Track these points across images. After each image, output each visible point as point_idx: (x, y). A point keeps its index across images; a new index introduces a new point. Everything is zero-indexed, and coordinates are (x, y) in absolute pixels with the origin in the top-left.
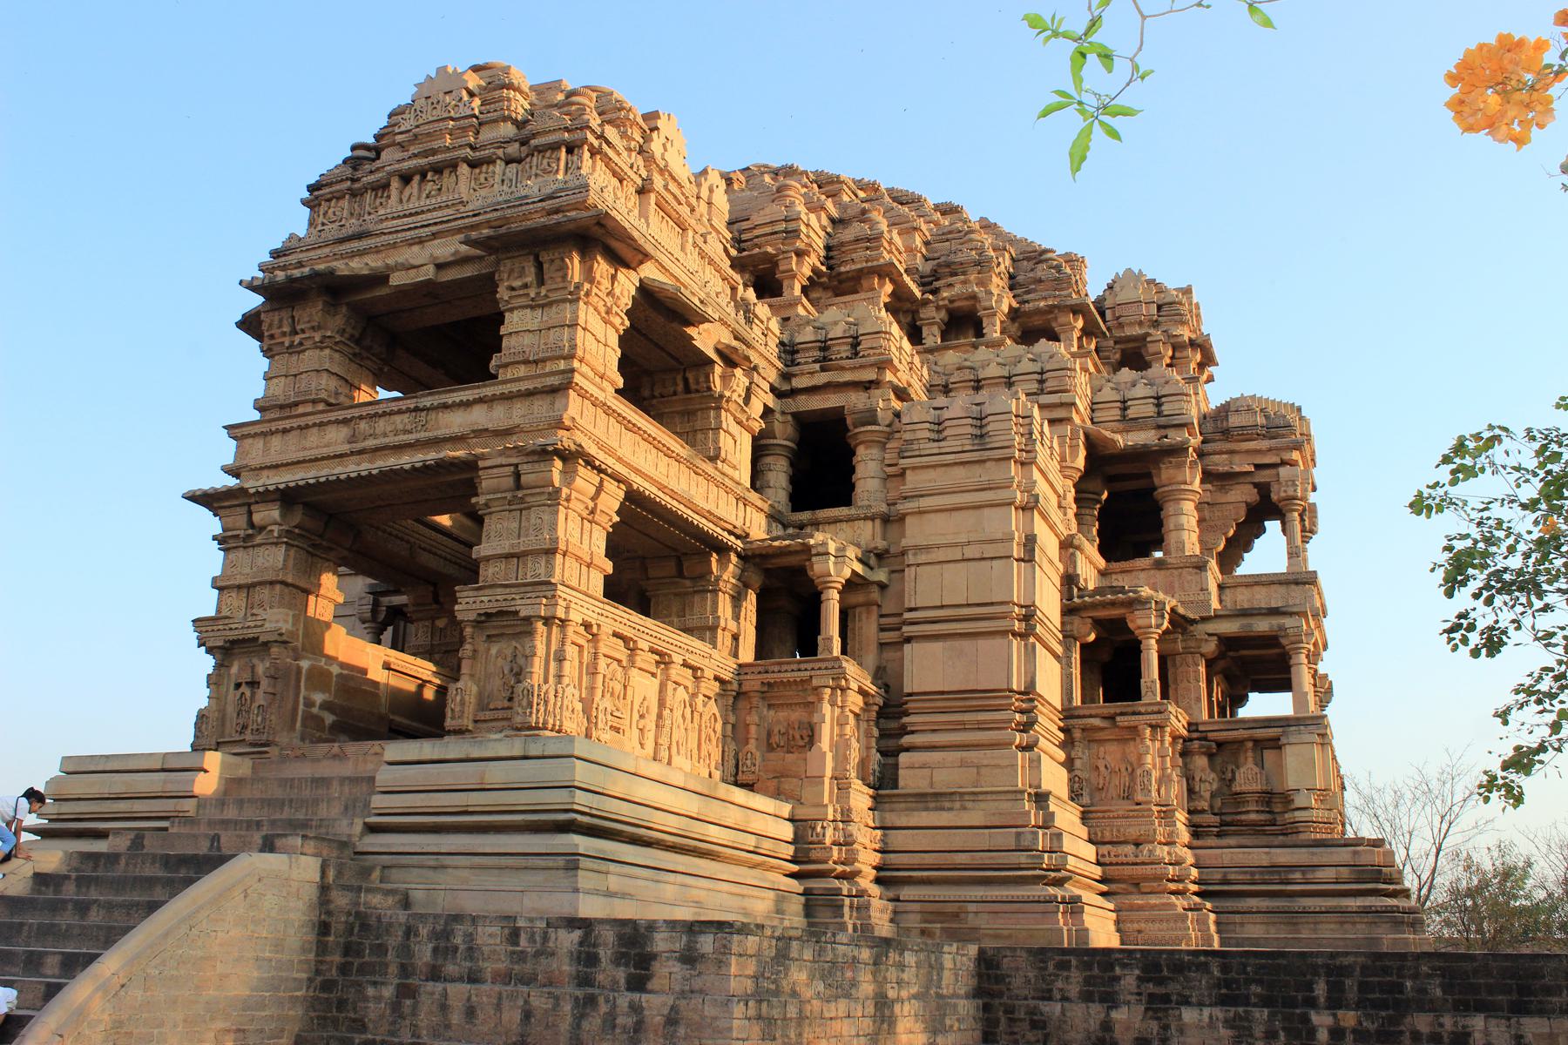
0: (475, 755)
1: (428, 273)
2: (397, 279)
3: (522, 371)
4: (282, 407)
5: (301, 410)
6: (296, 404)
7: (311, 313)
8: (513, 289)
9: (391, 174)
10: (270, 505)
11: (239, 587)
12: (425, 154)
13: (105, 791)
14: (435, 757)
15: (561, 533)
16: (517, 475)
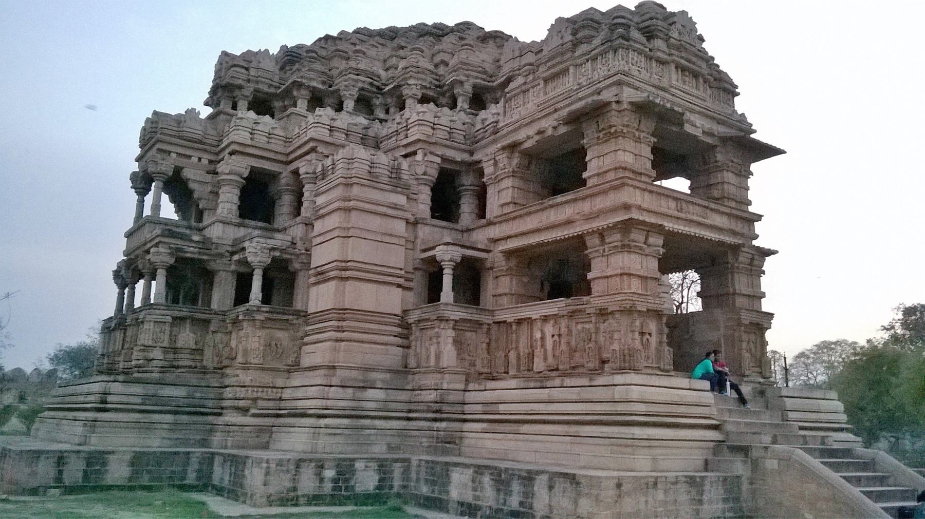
0: (810, 396)
1: (698, 133)
2: (688, 128)
3: (733, 204)
4: (633, 172)
5: (643, 178)
6: (641, 174)
7: (649, 125)
8: (732, 162)
9: (673, 61)
10: (658, 236)
11: (640, 277)
12: (689, 61)
13: (669, 399)
14: (796, 395)
15: (737, 287)
16: (752, 259)
